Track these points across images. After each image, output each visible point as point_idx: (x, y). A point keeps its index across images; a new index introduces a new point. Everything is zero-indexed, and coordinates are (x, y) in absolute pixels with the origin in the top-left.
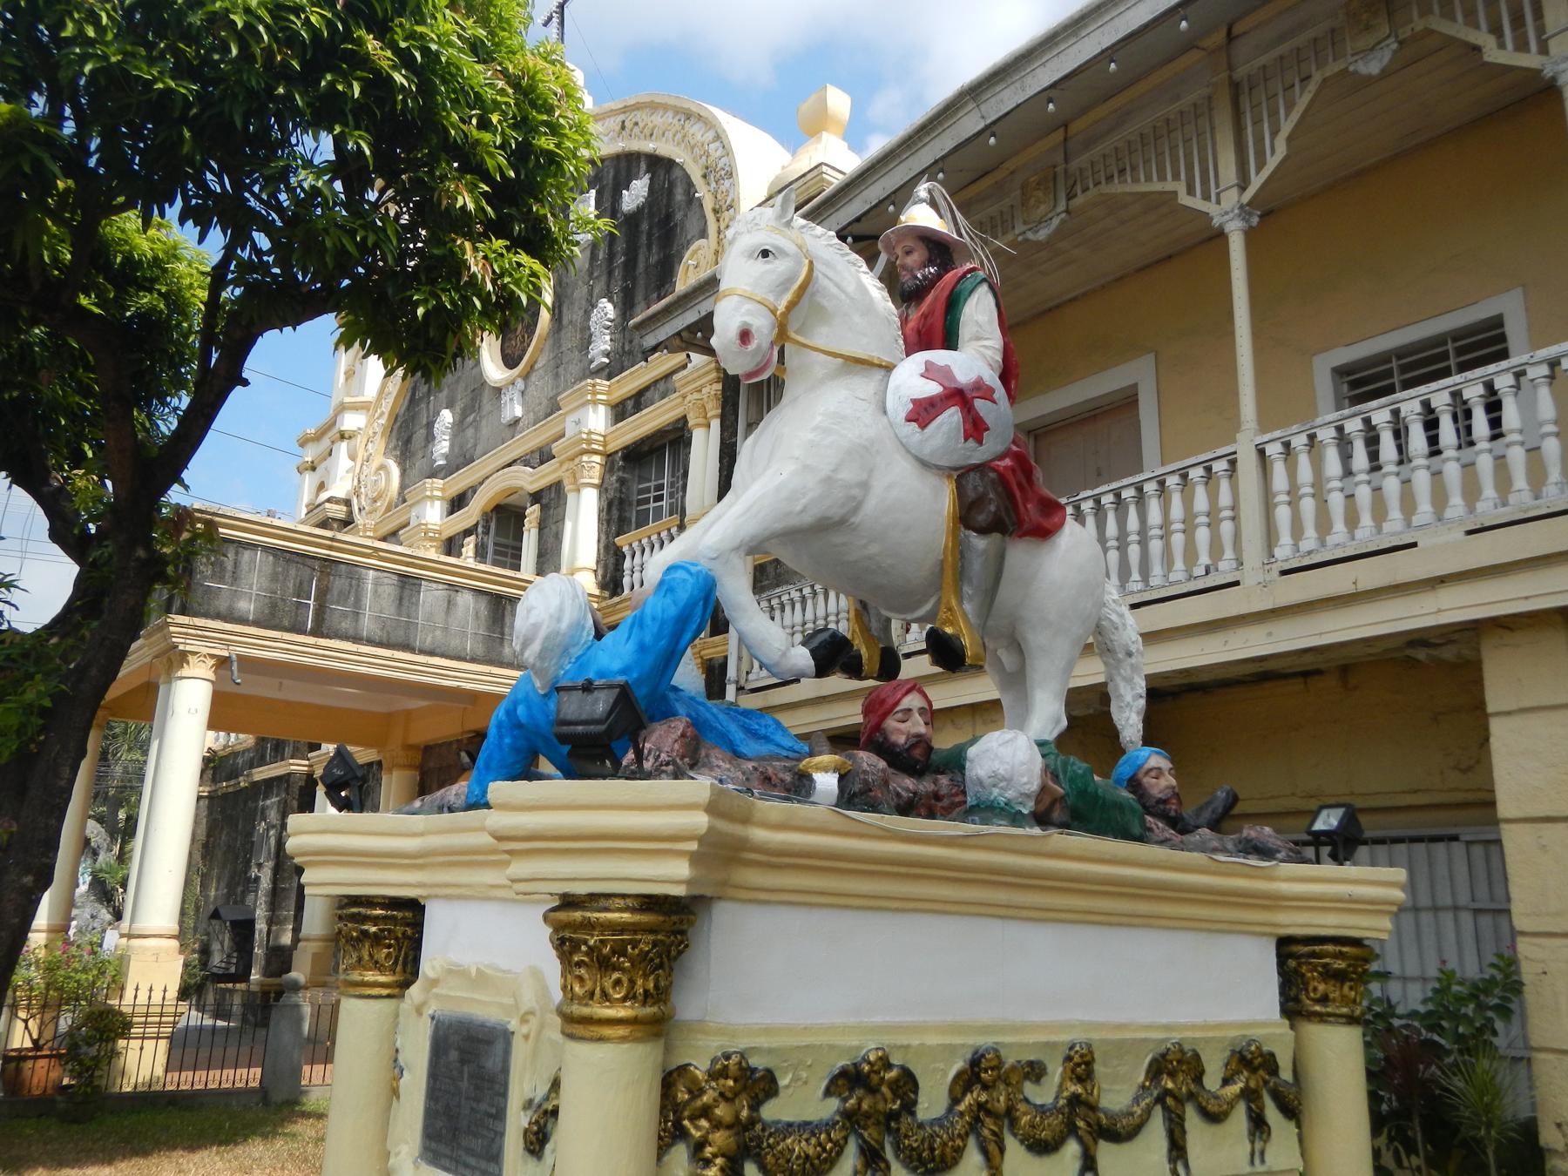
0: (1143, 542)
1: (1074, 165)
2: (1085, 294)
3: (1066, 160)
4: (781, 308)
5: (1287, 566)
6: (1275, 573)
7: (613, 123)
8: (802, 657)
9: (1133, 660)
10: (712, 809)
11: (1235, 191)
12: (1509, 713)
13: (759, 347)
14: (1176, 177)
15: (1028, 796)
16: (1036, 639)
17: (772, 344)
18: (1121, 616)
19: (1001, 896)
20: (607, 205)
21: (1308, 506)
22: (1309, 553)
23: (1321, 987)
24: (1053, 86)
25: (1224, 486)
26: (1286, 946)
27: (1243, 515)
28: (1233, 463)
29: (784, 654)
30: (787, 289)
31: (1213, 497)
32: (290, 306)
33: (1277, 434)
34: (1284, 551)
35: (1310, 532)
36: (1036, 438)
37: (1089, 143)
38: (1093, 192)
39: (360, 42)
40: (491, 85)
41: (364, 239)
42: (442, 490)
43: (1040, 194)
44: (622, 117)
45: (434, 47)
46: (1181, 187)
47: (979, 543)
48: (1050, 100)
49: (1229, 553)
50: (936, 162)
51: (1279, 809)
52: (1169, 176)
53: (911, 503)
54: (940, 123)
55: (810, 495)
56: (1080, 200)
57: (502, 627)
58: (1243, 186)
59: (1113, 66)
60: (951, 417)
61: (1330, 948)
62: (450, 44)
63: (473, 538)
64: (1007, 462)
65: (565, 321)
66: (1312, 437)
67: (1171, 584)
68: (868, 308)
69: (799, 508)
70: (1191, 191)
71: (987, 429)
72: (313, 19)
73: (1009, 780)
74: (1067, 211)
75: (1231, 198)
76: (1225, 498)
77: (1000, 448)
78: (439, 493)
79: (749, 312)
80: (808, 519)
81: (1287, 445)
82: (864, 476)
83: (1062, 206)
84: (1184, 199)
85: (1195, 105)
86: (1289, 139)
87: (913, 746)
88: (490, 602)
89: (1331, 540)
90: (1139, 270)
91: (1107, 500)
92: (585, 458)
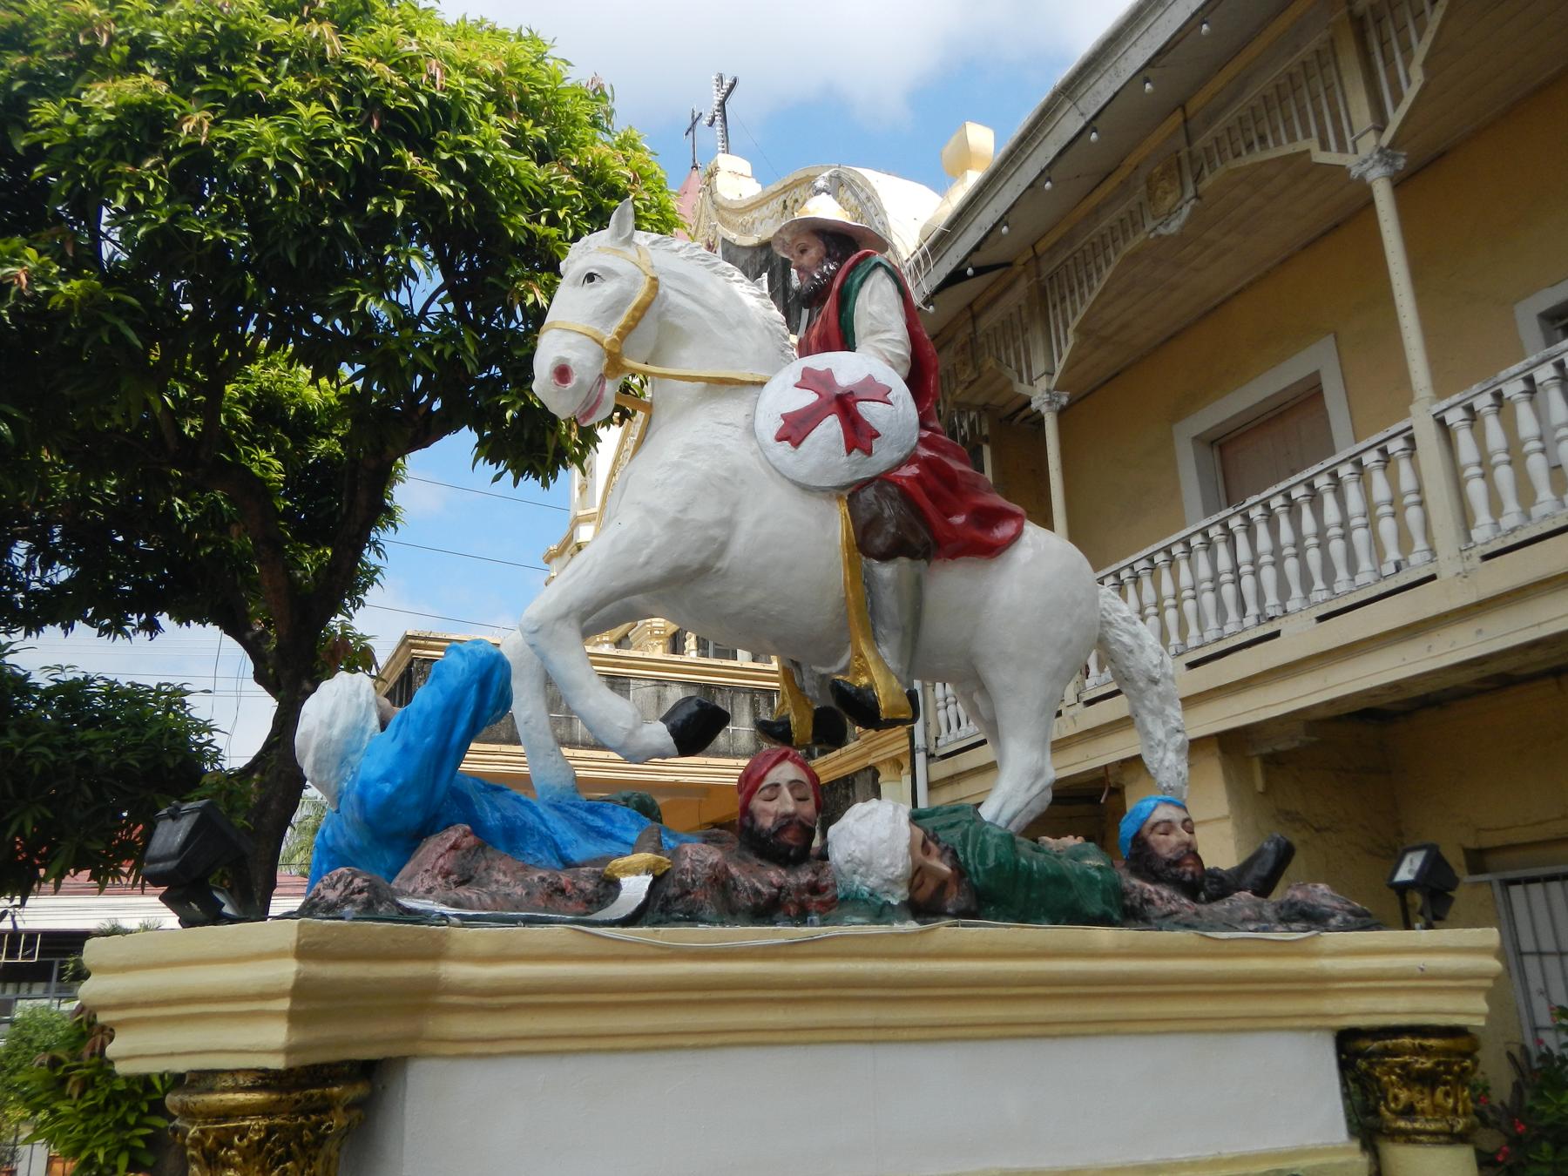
0: (1323, 545)
1: (1198, 144)
2: (1251, 284)
3: (1189, 143)
4: (609, 334)
5: (1489, 549)
6: (1476, 560)
7: (776, 205)
8: (658, 734)
9: (1160, 688)
10: (304, 952)
11: (1372, 134)
13: (580, 382)
14: (1307, 135)
15: (894, 882)
16: (999, 677)
17: (602, 379)
18: (1136, 636)
19: (865, 1015)
20: (779, 285)
21: (1504, 475)
22: (1513, 530)
23: (1404, 1095)
24: (1150, 63)
25: (1405, 467)
26: (1350, 1044)
27: (1429, 498)
28: (1411, 440)
29: (631, 733)
30: (619, 313)
31: (1393, 482)
32: (426, 432)
33: (1456, 398)
34: (1482, 532)
35: (1511, 505)
36: (1221, 448)
37: (1209, 120)
38: (1221, 169)
39: (400, 161)
40: (558, 181)
41: (441, 352)
43: (1165, 184)
44: (783, 197)
45: (479, 153)
46: (1313, 145)
47: (886, 572)
48: (1147, 80)
49: (1420, 544)
50: (1043, 172)
52: (1299, 135)
53: (793, 533)
54: (1040, 131)
55: (655, 543)
56: (1208, 181)
58: (1380, 126)
59: (1205, 27)
60: (831, 428)
61: (1407, 1041)
62: (496, 147)
64: (913, 470)
66: (1498, 395)
67: (1360, 588)
68: (743, 320)
69: (642, 560)
70: (1324, 146)
71: (878, 435)
72: (347, 148)
73: (868, 864)
75: (1368, 143)
76: (1407, 481)
77: (897, 455)
79: (569, 346)
80: (656, 571)
81: (1470, 409)
82: (726, 512)
83: (1190, 192)
84: (1320, 157)
85: (1317, 52)
86: (1426, 65)
87: (782, 829)
89: (1536, 511)
90: (1305, 247)
91: (1277, 502)
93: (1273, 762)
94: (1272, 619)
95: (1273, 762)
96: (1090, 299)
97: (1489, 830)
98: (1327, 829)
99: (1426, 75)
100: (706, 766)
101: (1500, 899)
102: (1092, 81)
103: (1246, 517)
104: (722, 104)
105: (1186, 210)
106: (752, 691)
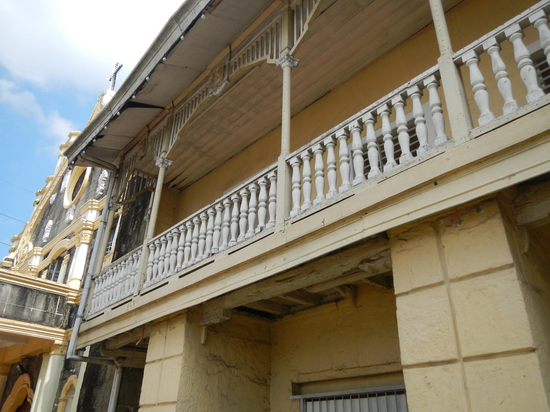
6: (290, 224)
11: (287, 50)
12: (407, 293)
22: (305, 211)
28: (276, 172)
42: (41, 252)
46: (267, 57)
51: (326, 378)
57: (25, 302)
63: (46, 271)
65: (92, 181)
70: (272, 57)
74: (228, 80)
78: (39, 253)
84: (270, 61)
86: (309, 24)
88: (20, 291)
89: (315, 202)
92: (84, 232)
93: (212, 329)
94: (213, 254)
95: (213, 330)
96: (186, 121)
97: (303, 374)
98: (233, 367)
99: (309, 28)
100: (13, 324)
101: (302, 408)
102: (186, 15)
103: (214, 209)
104: (116, 73)
105: (224, 85)
106: (48, 294)
